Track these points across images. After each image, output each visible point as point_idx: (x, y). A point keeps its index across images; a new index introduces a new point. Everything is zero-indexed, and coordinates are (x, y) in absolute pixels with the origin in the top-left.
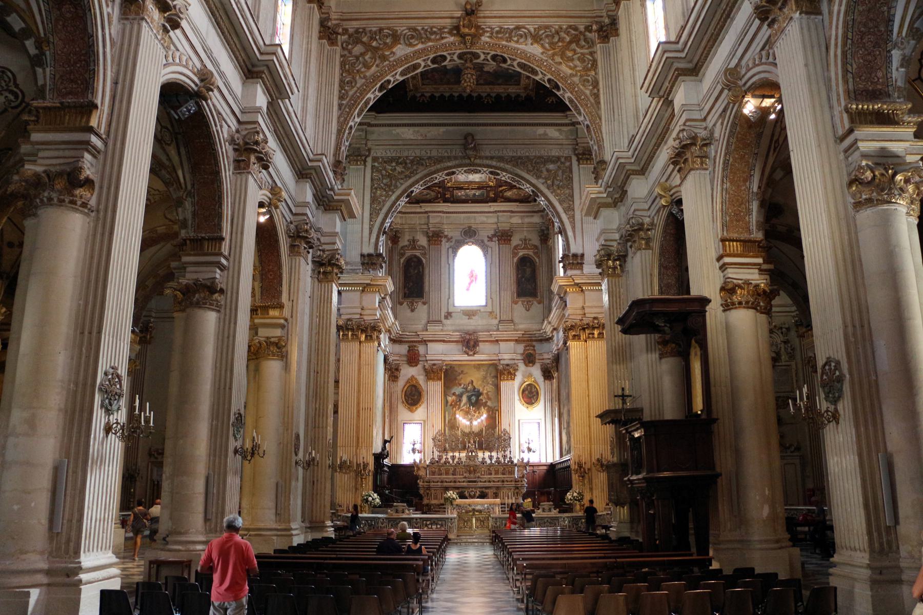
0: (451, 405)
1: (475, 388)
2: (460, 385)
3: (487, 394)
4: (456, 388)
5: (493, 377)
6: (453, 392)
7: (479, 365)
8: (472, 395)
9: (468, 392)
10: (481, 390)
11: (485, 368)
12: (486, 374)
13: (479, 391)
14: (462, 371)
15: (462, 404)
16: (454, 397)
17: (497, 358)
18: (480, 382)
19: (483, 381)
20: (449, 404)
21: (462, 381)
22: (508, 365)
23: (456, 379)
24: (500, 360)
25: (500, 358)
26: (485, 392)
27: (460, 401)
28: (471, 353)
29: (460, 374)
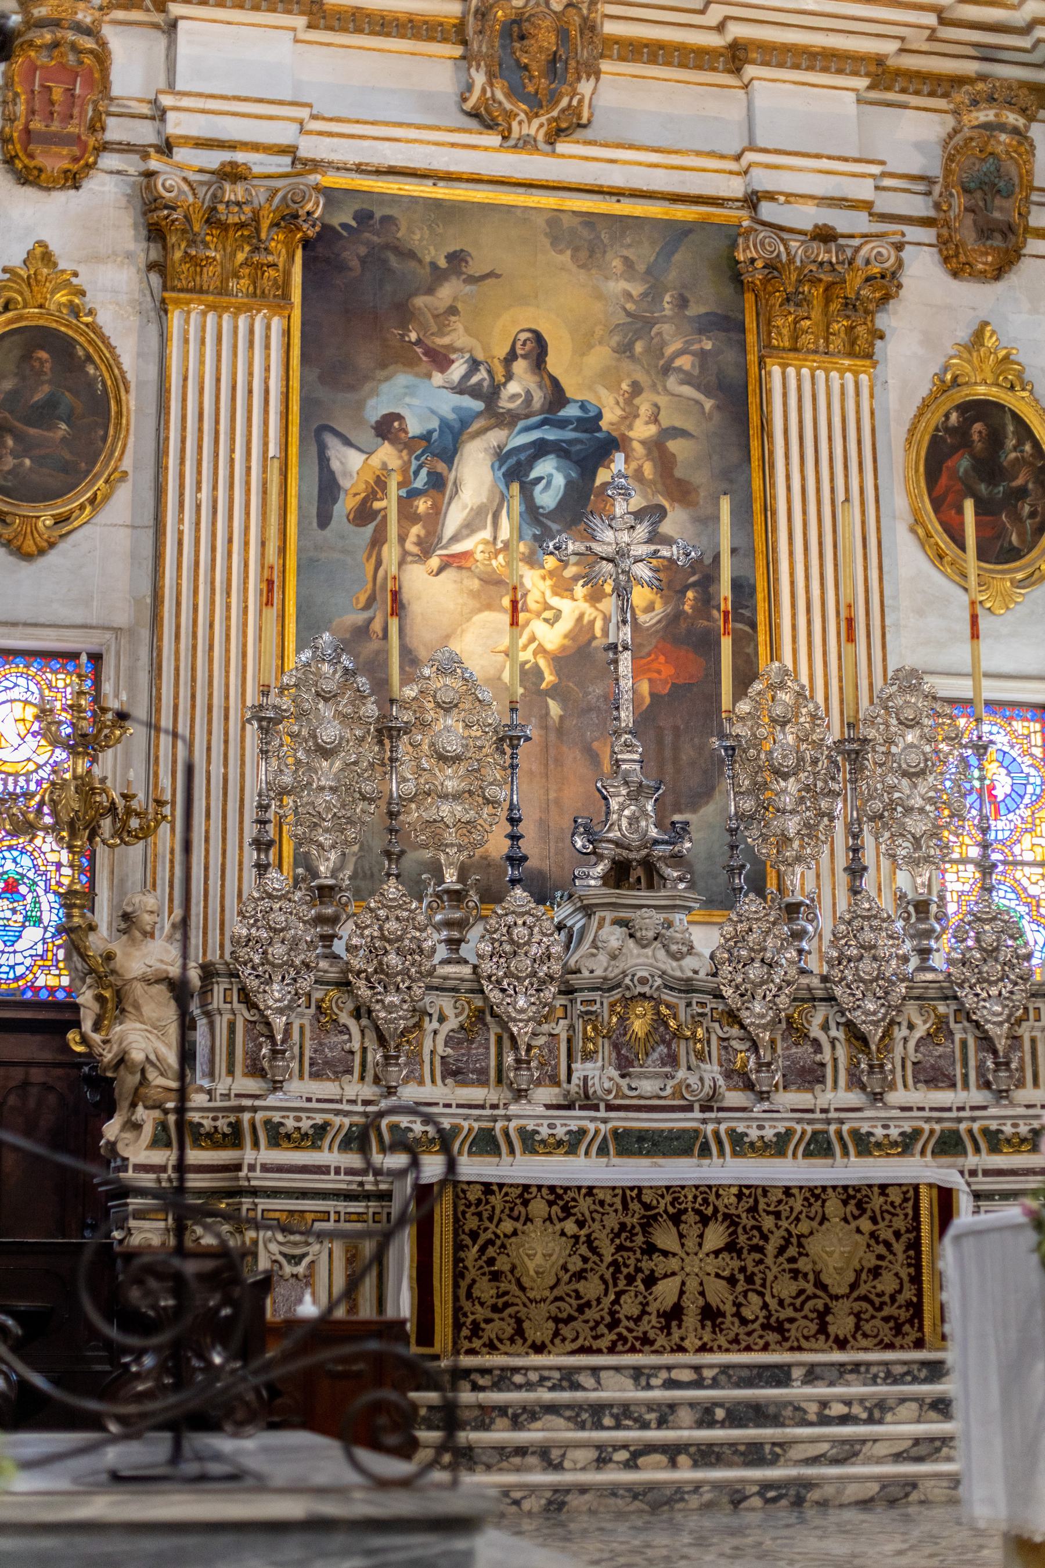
0: (364, 514)
1: (557, 396)
2: (441, 360)
3: (657, 448)
4: (402, 379)
5: (707, 325)
6: (376, 409)
7: (589, 219)
8: (541, 449)
9: (507, 420)
10: (610, 417)
11: (644, 254)
12: (653, 295)
13: (590, 422)
14: (456, 259)
15: (454, 518)
16: (387, 454)
17: (735, 187)
18: (600, 356)
19: (625, 350)
20: (346, 505)
21: (457, 336)
22: (825, 235)
23: (404, 314)
24: (752, 200)
25: (761, 180)
26: (642, 431)
27: (437, 483)
28: (536, 128)
29: (439, 276)
